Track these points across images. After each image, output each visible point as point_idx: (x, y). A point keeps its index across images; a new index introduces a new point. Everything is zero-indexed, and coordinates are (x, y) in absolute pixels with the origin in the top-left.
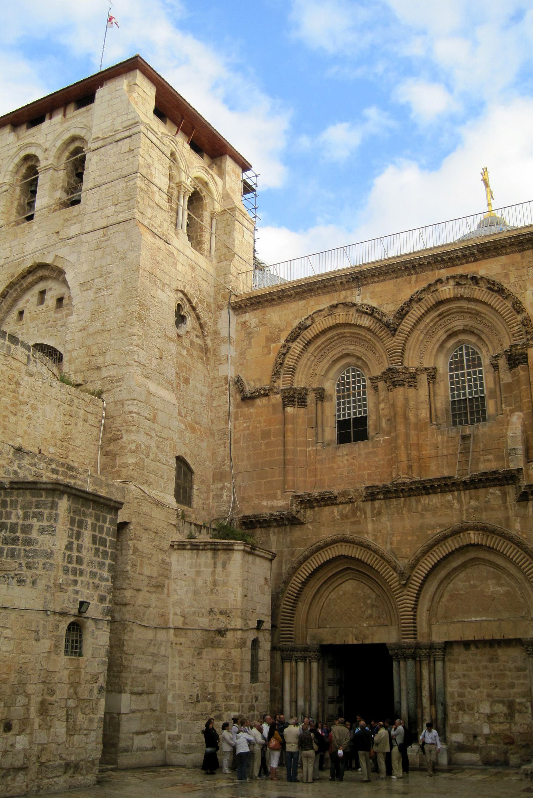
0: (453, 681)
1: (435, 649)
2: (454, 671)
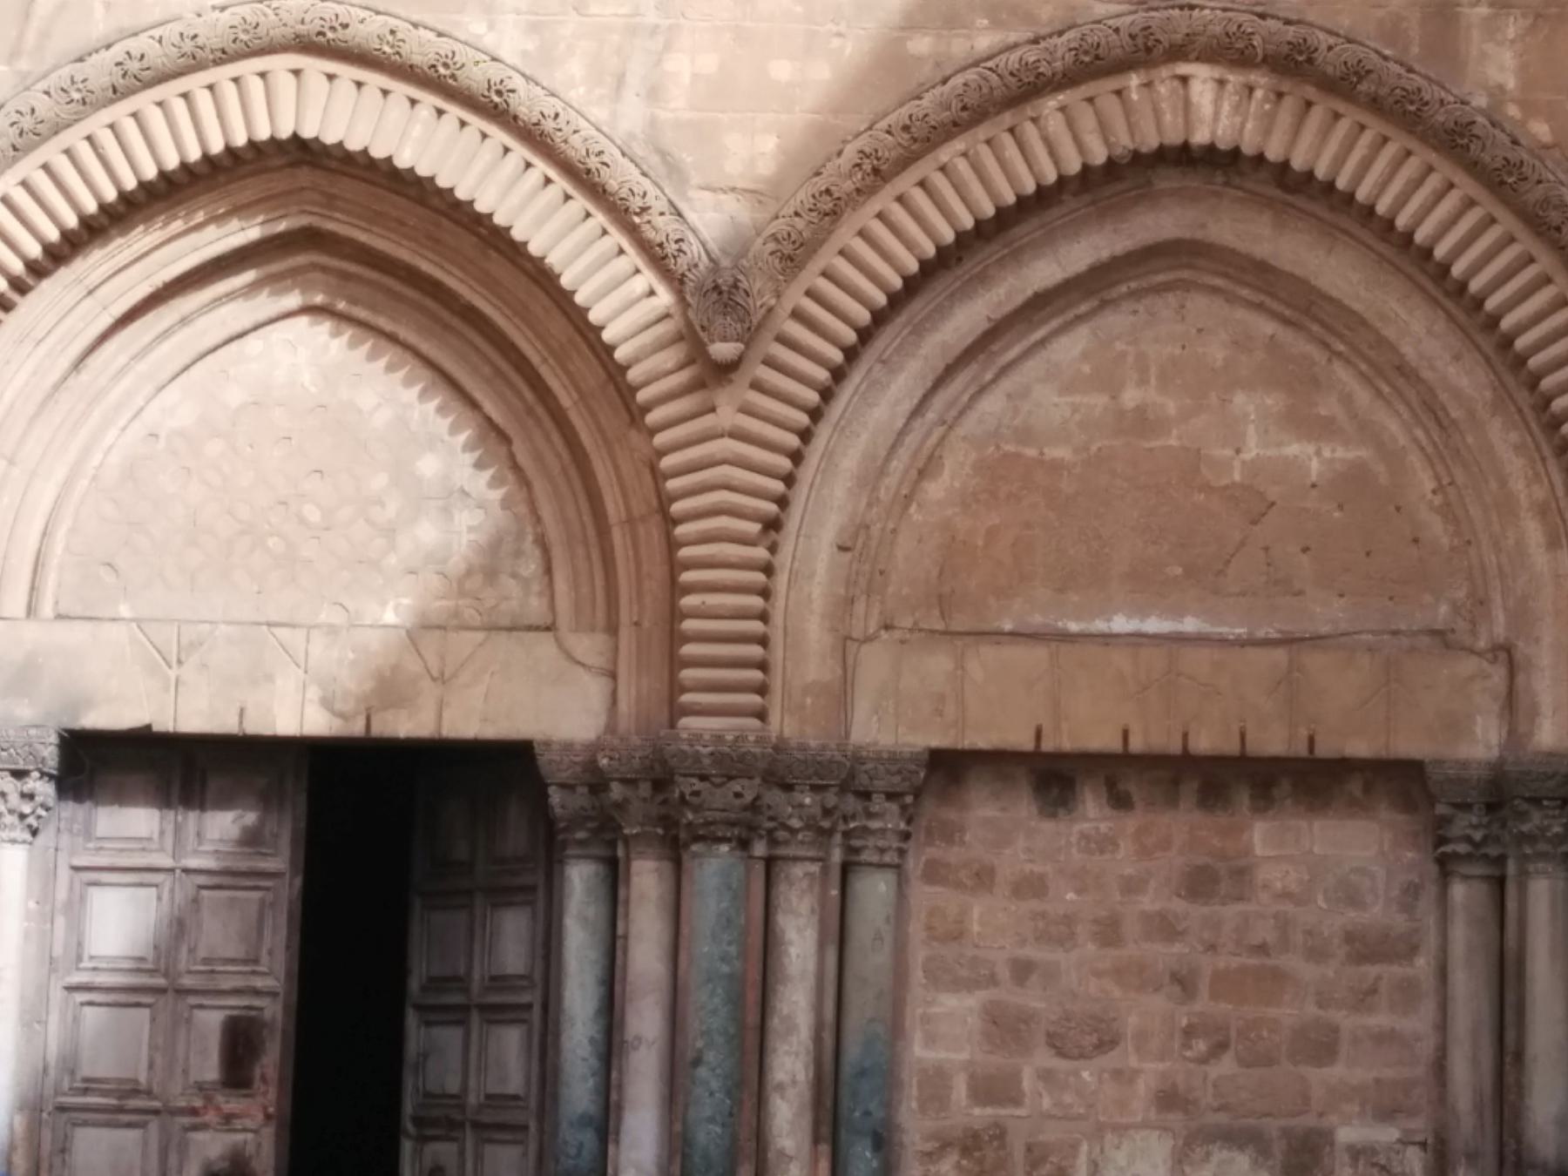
0: (949, 1002)
1: (866, 795)
2: (957, 935)
